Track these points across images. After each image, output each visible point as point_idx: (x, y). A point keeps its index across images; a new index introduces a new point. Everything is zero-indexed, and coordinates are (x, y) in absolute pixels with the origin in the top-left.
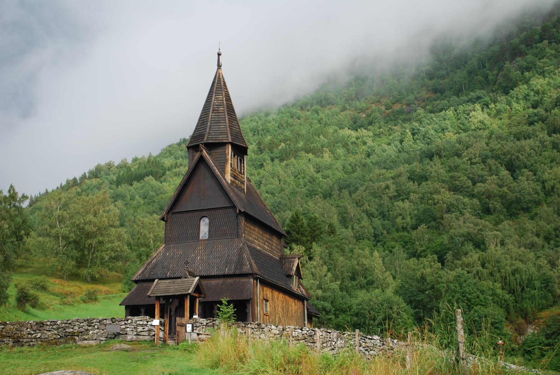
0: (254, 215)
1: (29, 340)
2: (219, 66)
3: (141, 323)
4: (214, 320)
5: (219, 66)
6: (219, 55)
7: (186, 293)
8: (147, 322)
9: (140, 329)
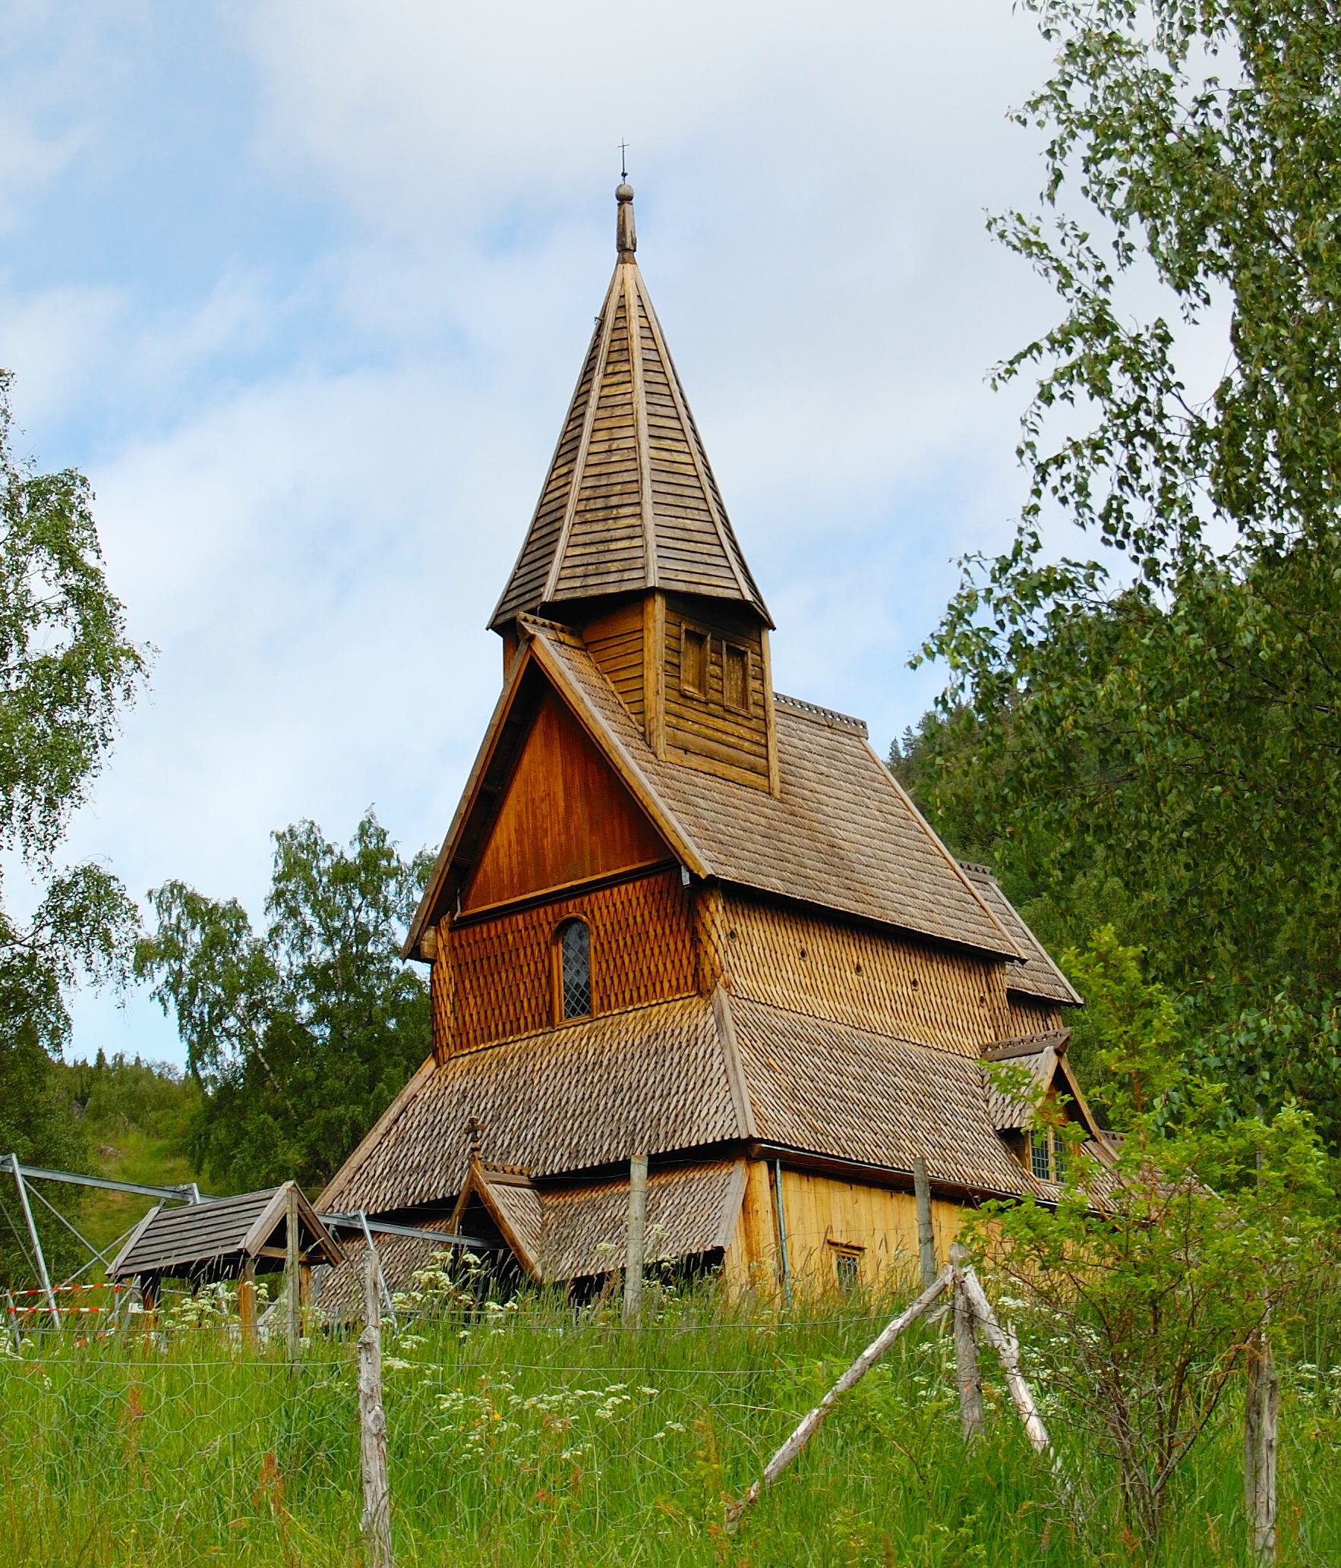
2: (625, 249)
5: (625, 249)
6: (624, 199)
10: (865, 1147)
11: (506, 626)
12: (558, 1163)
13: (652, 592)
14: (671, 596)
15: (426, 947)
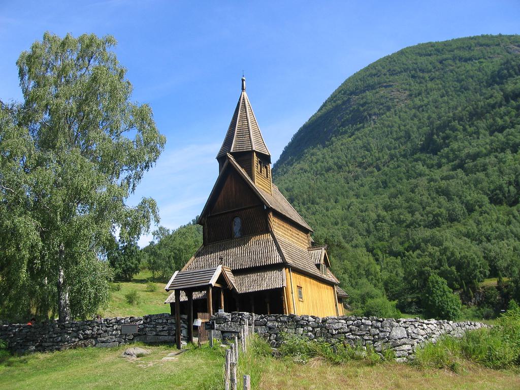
0: (281, 212)
1: (51, 344)
3: (160, 321)
4: (239, 315)
6: (243, 80)
7: (207, 284)
8: (167, 320)
9: (160, 328)
10: (300, 266)
11: (222, 158)
12: (238, 267)
13: (254, 151)
14: (256, 152)
15: (202, 221)
